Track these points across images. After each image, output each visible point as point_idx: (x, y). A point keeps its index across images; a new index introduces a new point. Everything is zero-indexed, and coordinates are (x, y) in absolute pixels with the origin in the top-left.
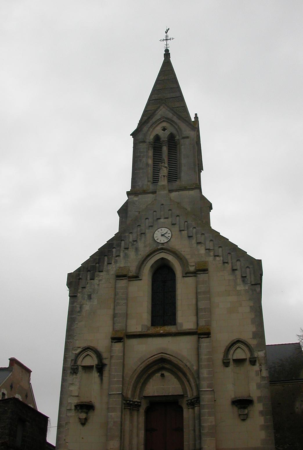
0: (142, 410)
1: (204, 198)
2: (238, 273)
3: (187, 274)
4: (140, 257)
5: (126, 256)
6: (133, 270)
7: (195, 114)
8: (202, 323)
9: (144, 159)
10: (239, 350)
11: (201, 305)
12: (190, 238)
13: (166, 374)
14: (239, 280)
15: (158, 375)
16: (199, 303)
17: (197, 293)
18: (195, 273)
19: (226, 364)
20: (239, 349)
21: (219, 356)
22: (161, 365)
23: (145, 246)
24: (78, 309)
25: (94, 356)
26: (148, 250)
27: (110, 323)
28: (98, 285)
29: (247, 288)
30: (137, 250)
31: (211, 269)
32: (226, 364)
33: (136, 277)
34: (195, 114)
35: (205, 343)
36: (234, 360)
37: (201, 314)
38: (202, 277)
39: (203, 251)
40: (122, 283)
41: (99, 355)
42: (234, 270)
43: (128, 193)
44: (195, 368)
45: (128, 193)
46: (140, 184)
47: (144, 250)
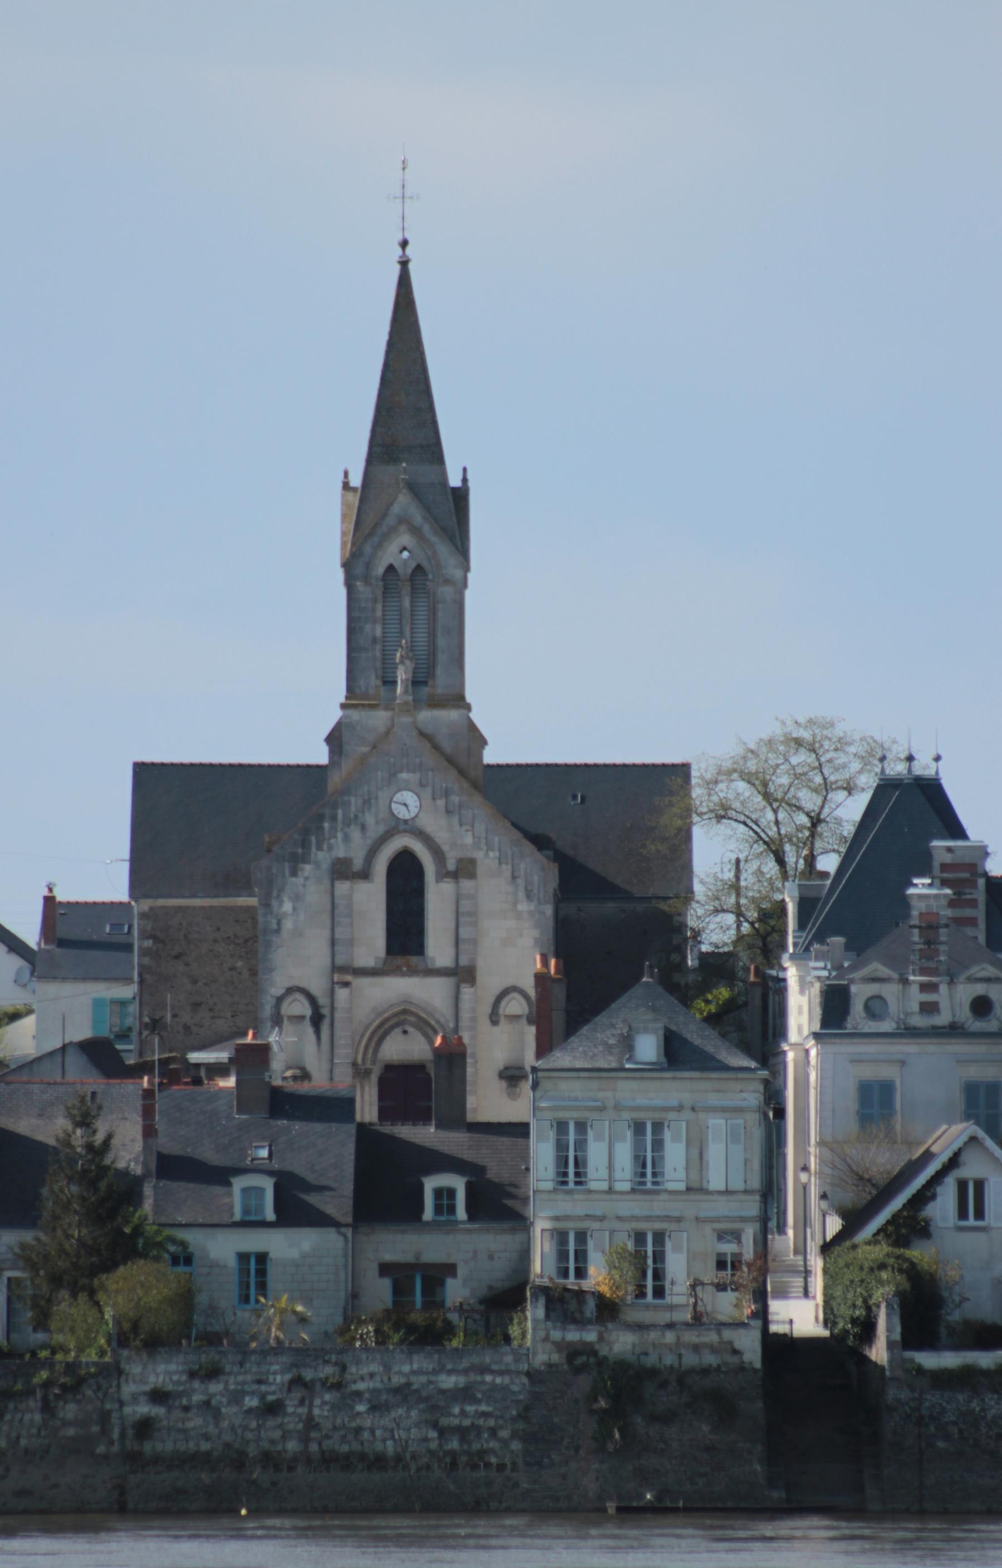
0: (374, 1078)
1: (472, 727)
2: (521, 882)
3: (444, 874)
4: (369, 842)
5: (347, 839)
6: (358, 864)
7: (526, 1125)
8: (464, 961)
9: (368, 627)
10: (514, 1002)
11: (464, 933)
12: (401, 548)
13: (410, 1029)
14: (521, 894)
15: (398, 1031)
16: (461, 930)
17: (457, 913)
18: (455, 875)
19: (494, 1018)
20: (514, 1001)
21: (486, 1009)
22: (402, 1017)
23: (377, 823)
24: (275, 926)
25: (306, 1003)
26: (381, 829)
27: (326, 951)
28: (304, 886)
29: (532, 908)
30: (363, 828)
31: (480, 870)
32: (494, 1018)
33: (365, 875)
34: (526, 1125)
35: (466, 991)
36: (506, 1016)
37: (462, 947)
38: (466, 884)
39: (469, 840)
40: (342, 887)
41: (312, 1000)
42: (514, 877)
43: (343, 706)
44: (452, 1025)
45: (343, 706)
46: (362, 683)
47: (376, 830)
